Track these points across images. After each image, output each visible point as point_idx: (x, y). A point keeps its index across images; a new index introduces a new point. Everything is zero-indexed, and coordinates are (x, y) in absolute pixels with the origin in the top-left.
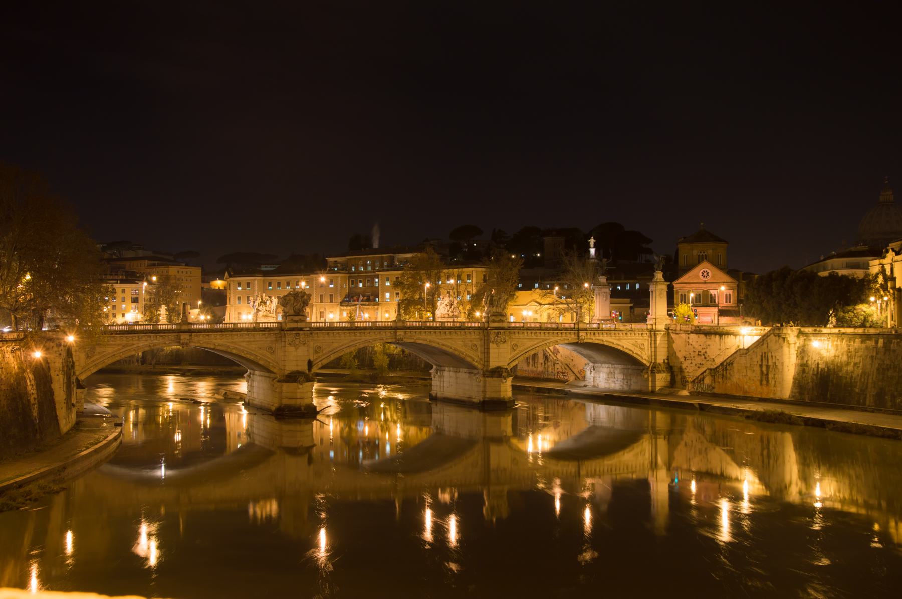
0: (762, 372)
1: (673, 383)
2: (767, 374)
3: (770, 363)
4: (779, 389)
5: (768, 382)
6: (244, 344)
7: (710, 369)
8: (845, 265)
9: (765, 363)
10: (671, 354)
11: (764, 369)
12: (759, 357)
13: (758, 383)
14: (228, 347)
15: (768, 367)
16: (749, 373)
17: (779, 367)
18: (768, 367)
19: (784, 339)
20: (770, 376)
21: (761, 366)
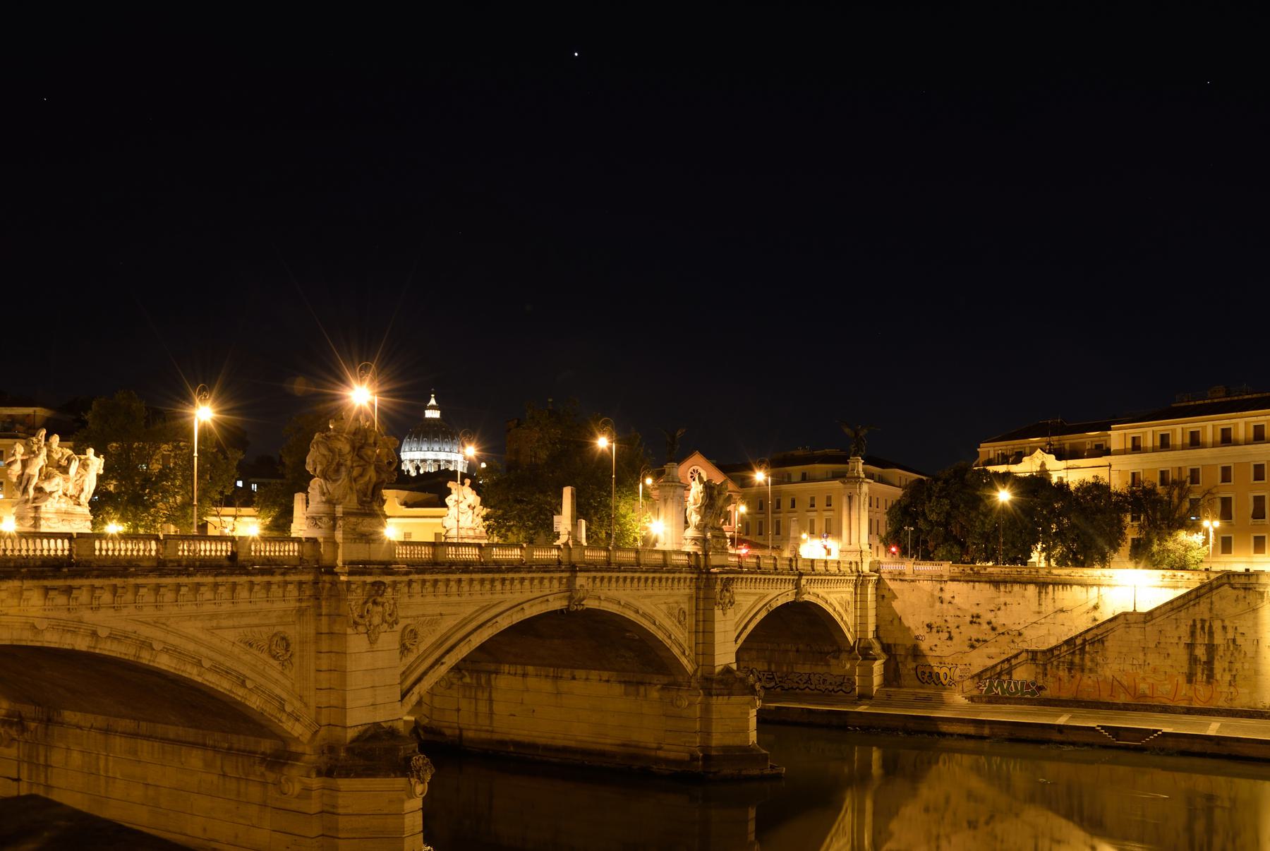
0: (1193, 660)
1: (892, 676)
2: (1209, 663)
3: (1219, 639)
4: (1244, 691)
5: (1210, 677)
6: (192, 628)
7: (1034, 653)
8: (830, 475)
9: (1202, 639)
10: (889, 620)
11: (1200, 652)
12: (1184, 630)
13: (1182, 680)
14: (146, 644)
15: (1211, 648)
16: (1154, 660)
17: (1246, 646)
18: (1211, 648)
19: (1262, 594)
20: (1218, 666)
21: (1190, 647)
